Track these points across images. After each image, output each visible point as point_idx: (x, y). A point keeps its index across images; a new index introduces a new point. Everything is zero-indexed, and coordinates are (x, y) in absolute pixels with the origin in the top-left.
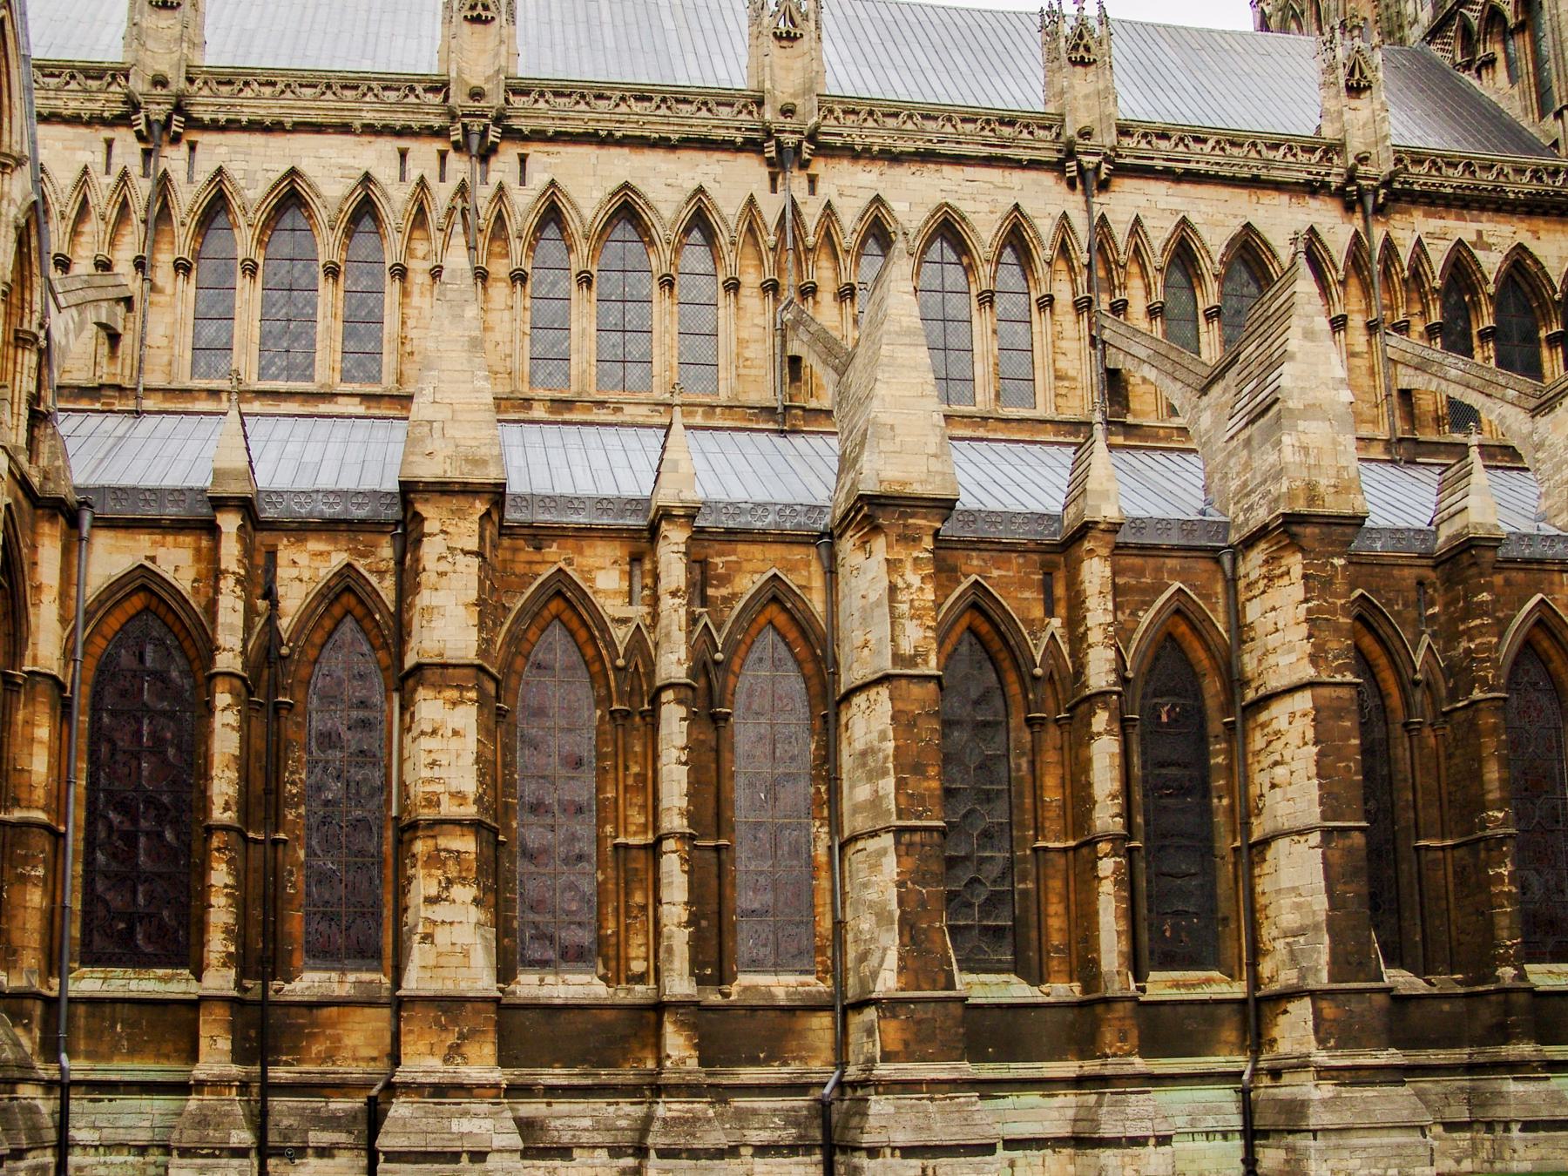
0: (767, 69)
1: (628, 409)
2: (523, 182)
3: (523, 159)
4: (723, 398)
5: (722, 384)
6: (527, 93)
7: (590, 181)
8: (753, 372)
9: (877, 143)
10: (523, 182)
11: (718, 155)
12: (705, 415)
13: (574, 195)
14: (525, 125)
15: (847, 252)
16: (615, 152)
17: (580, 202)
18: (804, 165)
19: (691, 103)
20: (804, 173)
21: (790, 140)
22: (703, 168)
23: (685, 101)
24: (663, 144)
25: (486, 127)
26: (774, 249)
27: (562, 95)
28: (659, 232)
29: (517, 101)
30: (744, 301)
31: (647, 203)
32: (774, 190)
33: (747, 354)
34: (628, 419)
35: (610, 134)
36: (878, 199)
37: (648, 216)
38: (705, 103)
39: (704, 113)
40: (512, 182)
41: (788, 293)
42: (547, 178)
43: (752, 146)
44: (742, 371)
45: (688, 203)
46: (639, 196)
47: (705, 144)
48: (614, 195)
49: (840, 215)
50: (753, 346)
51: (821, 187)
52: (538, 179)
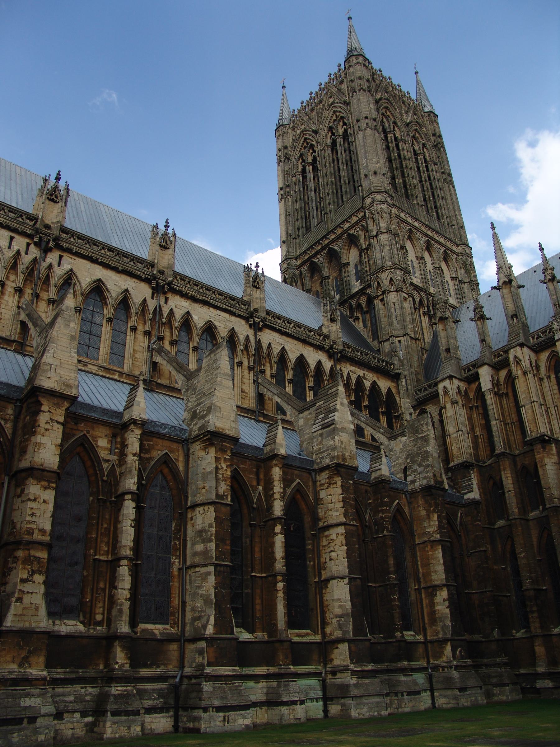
0: (157, 256)
1: (89, 366)
2: (59, 265)
3: (61, 257)
4: (126, 369)
5: (125, 366)
6: (67, 234)
7: (86, 274)
8: (138, 363)
9: (191, 293)
10: (59, 265)
11: (134, 280)
12: (119, 376)
13: (79, 276)
14: (65, 245)
15: (176, 328)
16: (97, 266)
17: (81, 281)
18: (165, 293)
19: (128, 258)
20: (164, 296)
21: (162, 283)
22: (128, 282)
23: (126, 257)
24: (115, 269)
25: (49, 241)
26: (151, 320)
27: (81, 239)
28: (110, 301)
29: (64, 236)
30: (137, 336)
31: (107, 289)
32: (153, 298)
33: (136, 356)
34: (89, 370)
35: (97, 259)
36: (188, 313)
37: (106, 294)
38: (133, 260)
39: (132, 263)
40: (55, 264)
41: (154, 339)
42: (69, 267)
43: (147, 281)
44: (134, 362)
45: (122, 294)
46: (104, 286)
47: (131, 275)
48: (95, 282)
49: (175, 315)
50: (139, 354)
51: (170, 302)
52: (66, 266)
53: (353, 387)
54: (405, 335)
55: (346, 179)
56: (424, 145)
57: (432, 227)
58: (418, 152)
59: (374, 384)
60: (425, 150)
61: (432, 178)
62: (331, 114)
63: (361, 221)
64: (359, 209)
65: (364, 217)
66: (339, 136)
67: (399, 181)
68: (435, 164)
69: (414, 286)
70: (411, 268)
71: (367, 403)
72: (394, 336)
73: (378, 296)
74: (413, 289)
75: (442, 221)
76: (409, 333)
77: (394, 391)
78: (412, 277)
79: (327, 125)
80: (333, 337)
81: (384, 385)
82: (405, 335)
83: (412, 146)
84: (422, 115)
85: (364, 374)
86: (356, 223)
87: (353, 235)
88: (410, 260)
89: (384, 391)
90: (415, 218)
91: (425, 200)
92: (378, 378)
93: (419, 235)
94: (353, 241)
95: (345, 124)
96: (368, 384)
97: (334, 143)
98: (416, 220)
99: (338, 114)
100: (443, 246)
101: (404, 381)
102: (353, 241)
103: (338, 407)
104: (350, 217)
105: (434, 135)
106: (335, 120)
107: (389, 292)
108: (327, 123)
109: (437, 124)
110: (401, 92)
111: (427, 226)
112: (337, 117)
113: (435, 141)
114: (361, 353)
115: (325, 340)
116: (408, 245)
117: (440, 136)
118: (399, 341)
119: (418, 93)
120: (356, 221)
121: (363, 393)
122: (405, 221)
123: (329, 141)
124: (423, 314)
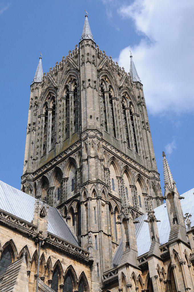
53: (52, 269)
54: (100, 231)
55: (73, 120)
56: (131, 103)
57: (131, 157)
58: (126, 107)
59: (71, 268)
60: (131, 106)
61: (135, 125)
62: (68, 77)
63: (79, 149)
64: (78, 141)
65: (81, 146)
66: (72, 92)
67: (110, 125)
68: (138, 116)
69: (112, 197)
70: (111, 184)
71: (62, 283)
72: (91, 232)
73: (84, 202)
74: (111, 199)
75: (139, 154)
76: (104, 230)
77: (87, 275)
78: (112, 190)
79: (64, 84)
80: (40, 229)
81: (79, 269)
82: (100, 231)
83: (121, 103)
84: (131, 83)
85: (63, 259)
86: (75, 151)
87: (72, 158)
88: (111, 178)
89: (78, 274)
90: (118, 150)
91: (128, 139)
92: (75, 263)
93: (120, 161)
94: (72, 163)
95: (76, 84)
96: (65, 268)
97: (68, 96)
98: (119, 151)
99: (72, 77)
100: (138, 171)
101: (96, 267)
102: (72, 163)
103: (18, 280)
104: (72, 146)
105: (139, 97)
106: (70, 81)
107: (91, 199)
108: (65, 83)
109: (142, 90)
110: (118, 67)
111: (126, 156)
112: (71, 79)
113: (139, 101)
114: (63, 242)
115: (33, 230)
116: (111, 168)
117: (143, 98)
118: (96, 236)
119: (131, 70)
120: (76, 149)
121: (60, 275)
122: (110, 151)
123: (65, 94)
124: (118, 218)
